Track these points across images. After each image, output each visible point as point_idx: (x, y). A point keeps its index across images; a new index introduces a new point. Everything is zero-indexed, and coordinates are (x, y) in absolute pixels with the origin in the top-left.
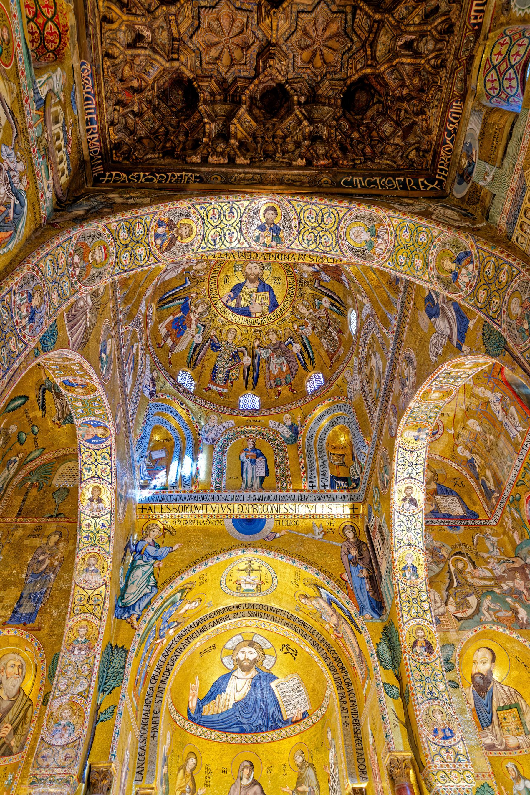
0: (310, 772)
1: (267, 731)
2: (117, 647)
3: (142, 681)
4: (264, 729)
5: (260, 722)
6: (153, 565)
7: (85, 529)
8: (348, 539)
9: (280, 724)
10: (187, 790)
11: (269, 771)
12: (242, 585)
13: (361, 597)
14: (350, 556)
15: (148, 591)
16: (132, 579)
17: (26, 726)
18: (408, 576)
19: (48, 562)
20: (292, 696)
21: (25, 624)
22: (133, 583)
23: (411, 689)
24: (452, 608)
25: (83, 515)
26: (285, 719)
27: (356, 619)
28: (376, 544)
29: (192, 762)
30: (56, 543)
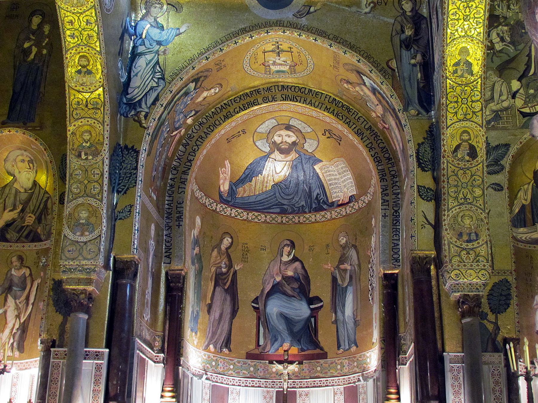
0: (353, 253)
1: (310, 212)
2: (126, 147)
3: (159, 175)
4: (307, 210)
5: (303, 203)
6: (157, 52)
7: (68, 27)
8: (404, 12)
9: (325, 207)
10: (223, 265)
11: (311, 249)
12: (272, 67)
13: (409, 89)
14: (403, 37)
16: (134, 71)
18: (459, 73)
19: (34, 50)
20: (338, 179)
21: (25, 124)
22: (136, 75)
23: (444, 194)
24: (519, 102)
26: (330, 201)
27: (400, 115)
28: (434, 26)
29: (227, 241)
30: (40, 26)
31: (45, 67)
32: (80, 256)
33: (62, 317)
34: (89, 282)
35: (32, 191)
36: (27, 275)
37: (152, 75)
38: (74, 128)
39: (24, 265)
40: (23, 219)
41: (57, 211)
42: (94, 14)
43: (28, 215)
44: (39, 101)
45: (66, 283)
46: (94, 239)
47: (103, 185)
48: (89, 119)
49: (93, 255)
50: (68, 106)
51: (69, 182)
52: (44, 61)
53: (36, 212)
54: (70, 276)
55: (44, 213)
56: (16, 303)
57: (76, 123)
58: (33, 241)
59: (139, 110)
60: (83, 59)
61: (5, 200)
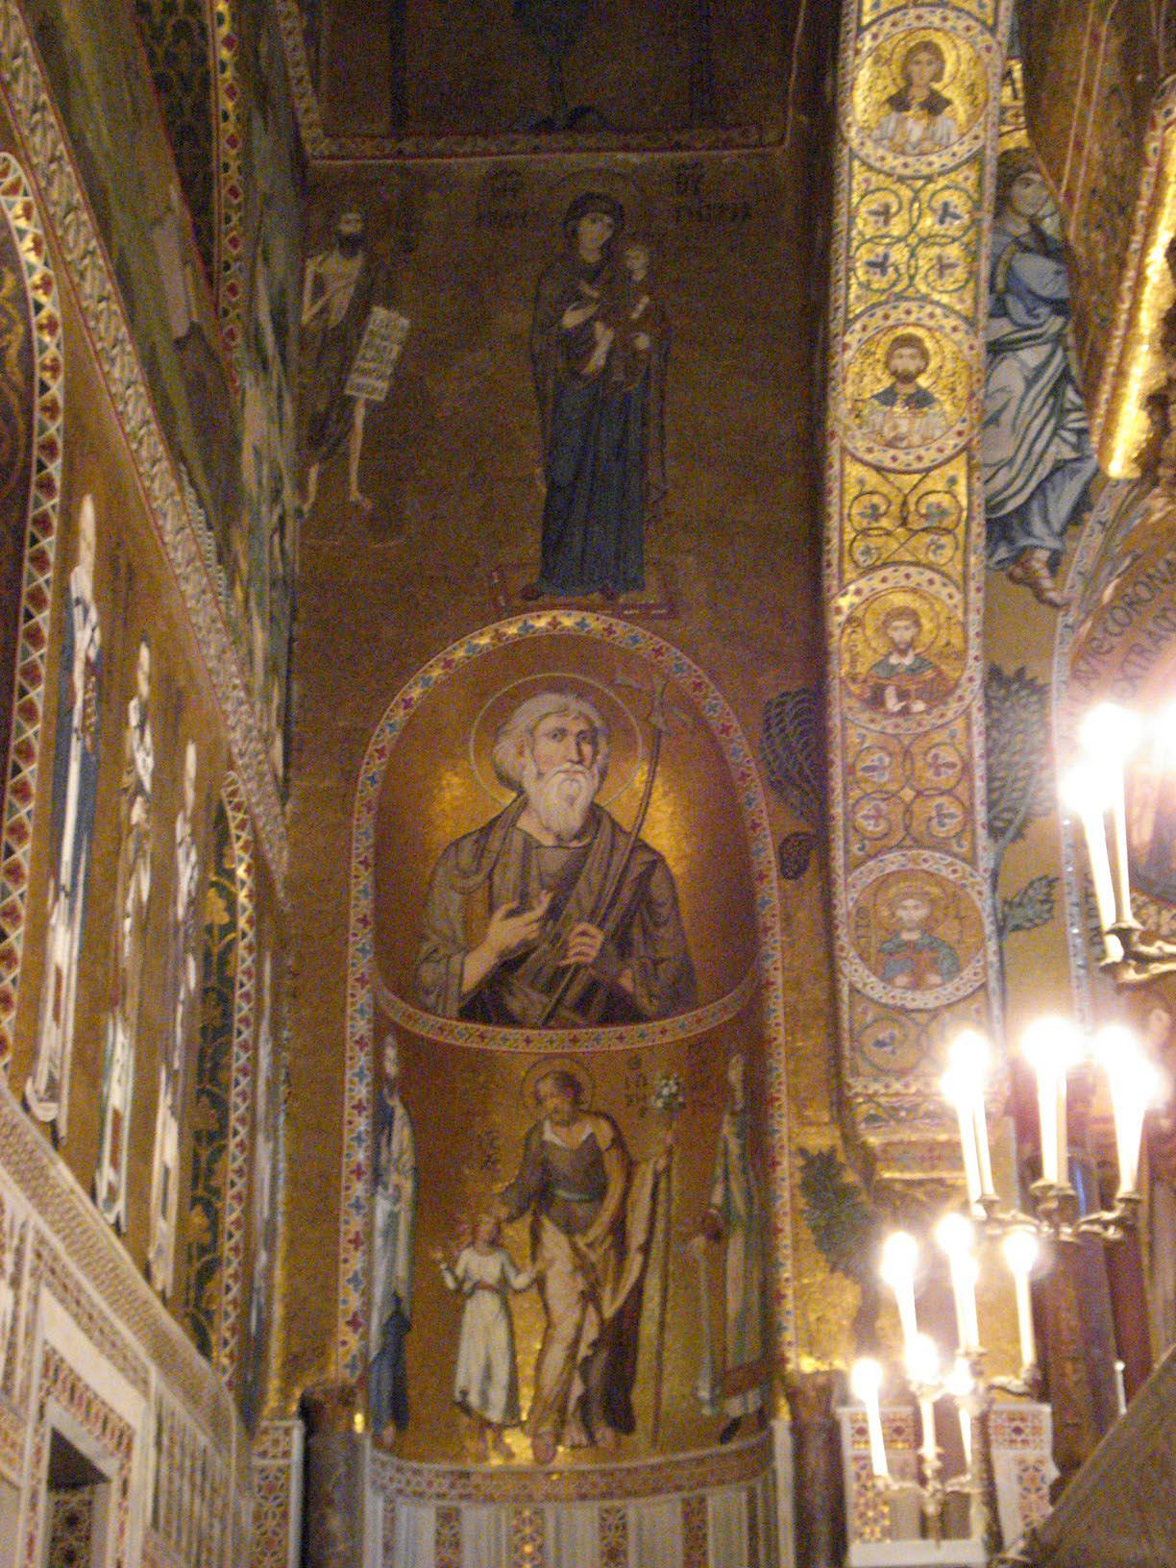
15: (1068, 453)
19: (604, 336)
25: (860, 174)
30: (610, 251)
31: (654, 393)
35: (586, 841)
37: (1053, 422)
38: (856, 600)
39: (584, 1107)
40: (559, 943)
41: (775, 901)
42: (969, 185)
43: (580, 927)
45: (886, 1160)
47: (972, 805)
48: (912, 570)
50: (834, 522)
52: (647, 376)
53: (604, 919)
54: (896, 1138)
55: (636, 922)
56: (574, 1247)
57: (862, 583)
58: (607, 1019)
59: (1024, 542)
60: (907, 351)
61: (490, 877)
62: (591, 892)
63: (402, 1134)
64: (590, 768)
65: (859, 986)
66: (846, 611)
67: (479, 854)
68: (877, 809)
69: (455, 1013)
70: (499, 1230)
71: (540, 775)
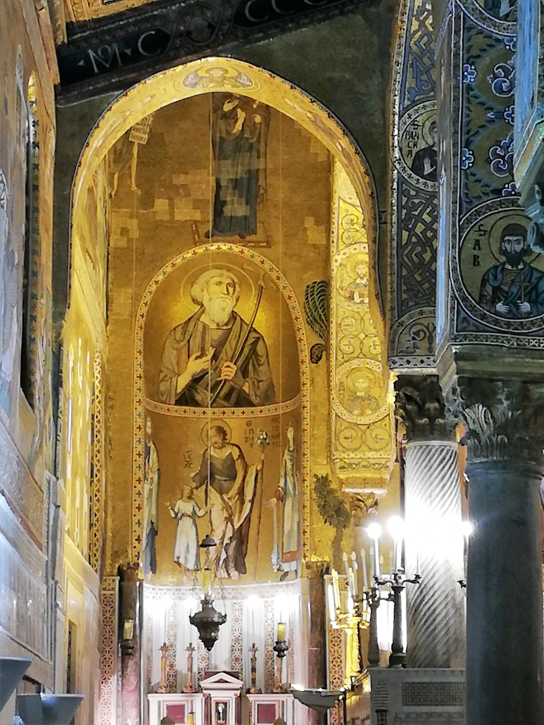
17: (263, 369)
19: (241, 115)
21: (242, 237)
31: (262, 144)
32: (363, 446)
33: (335, 529)
34: (380, 483)
35: (229, 327)
36: (236, 456)
38: (344, 257)
40: (217, 370)
41: (308, 373)
44: (259, 200)
46: (380, 420)
49: (383, 444)
51: (337, 337)
53: (237, 360)
54: (351, 476)
56: (223, 499)
57: (346, 250)
58: (237, 404)
61: (189, 341)
62: (231, 348)
63: (153, 455)
64: (232, 297)
65: (339, 415)
66: (339, 261)
67: (184, 333)
68: (349, 341)
69: (174, 402)
70: (192, 492)
71: (211, 299)
